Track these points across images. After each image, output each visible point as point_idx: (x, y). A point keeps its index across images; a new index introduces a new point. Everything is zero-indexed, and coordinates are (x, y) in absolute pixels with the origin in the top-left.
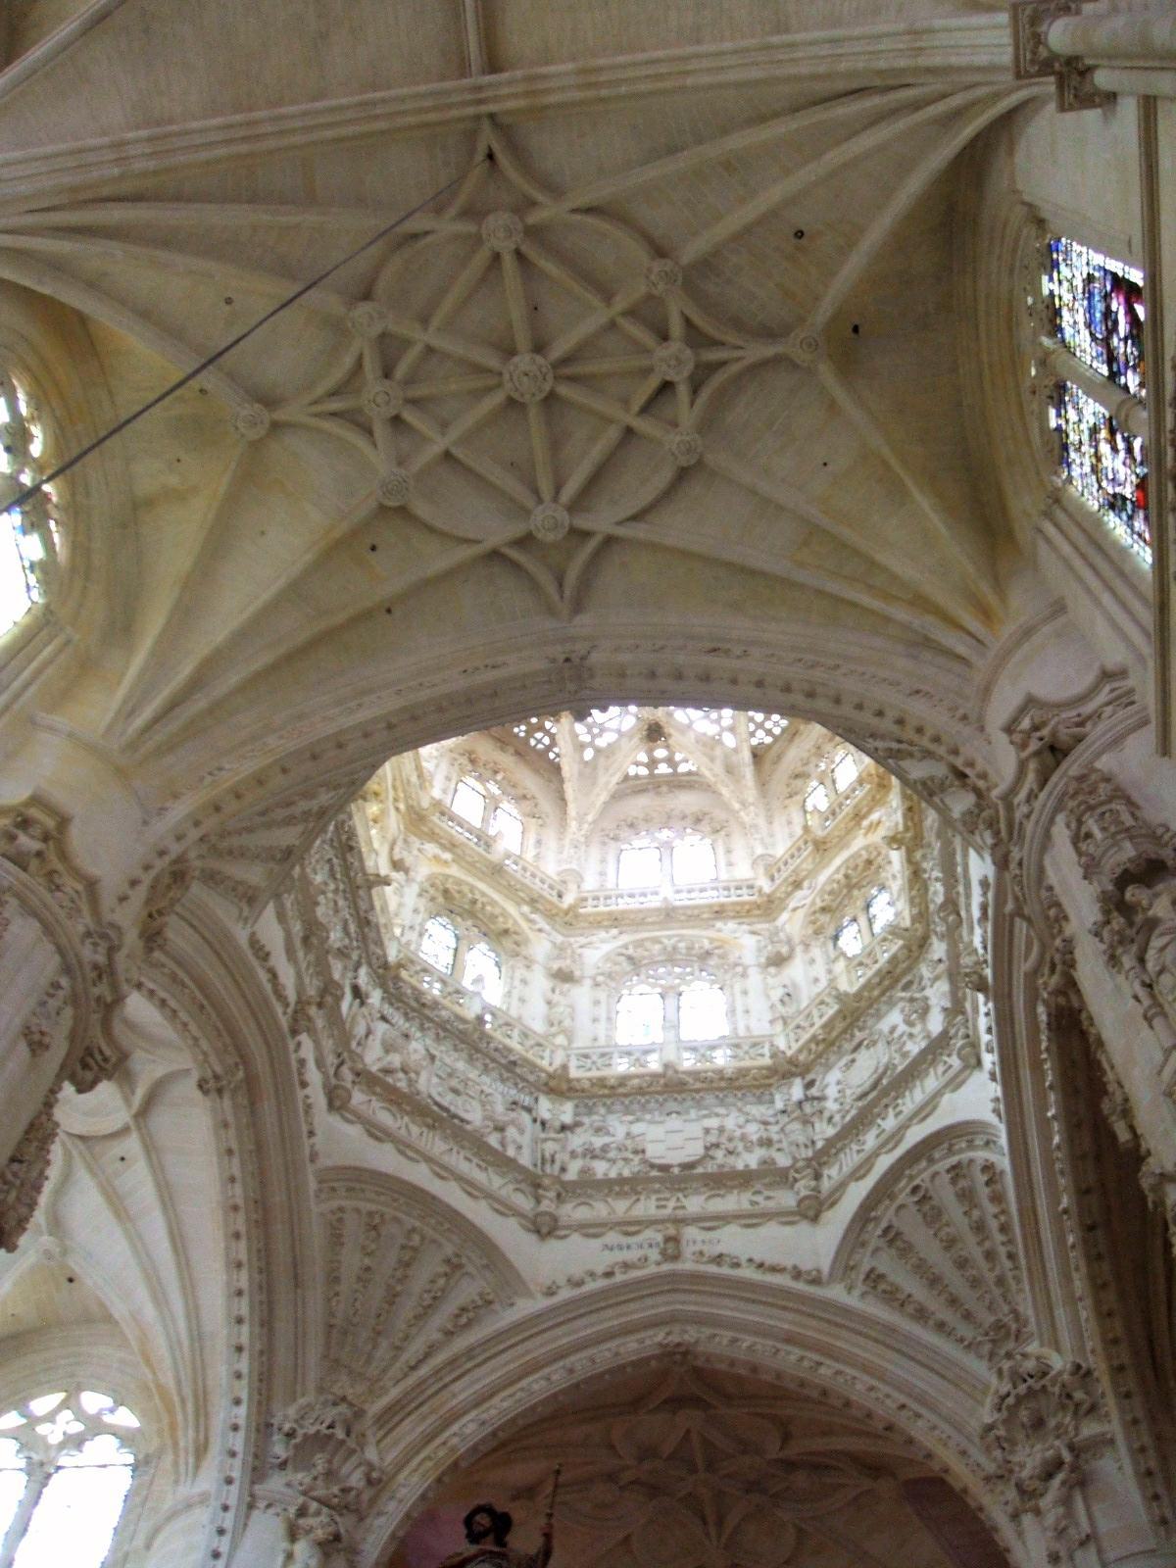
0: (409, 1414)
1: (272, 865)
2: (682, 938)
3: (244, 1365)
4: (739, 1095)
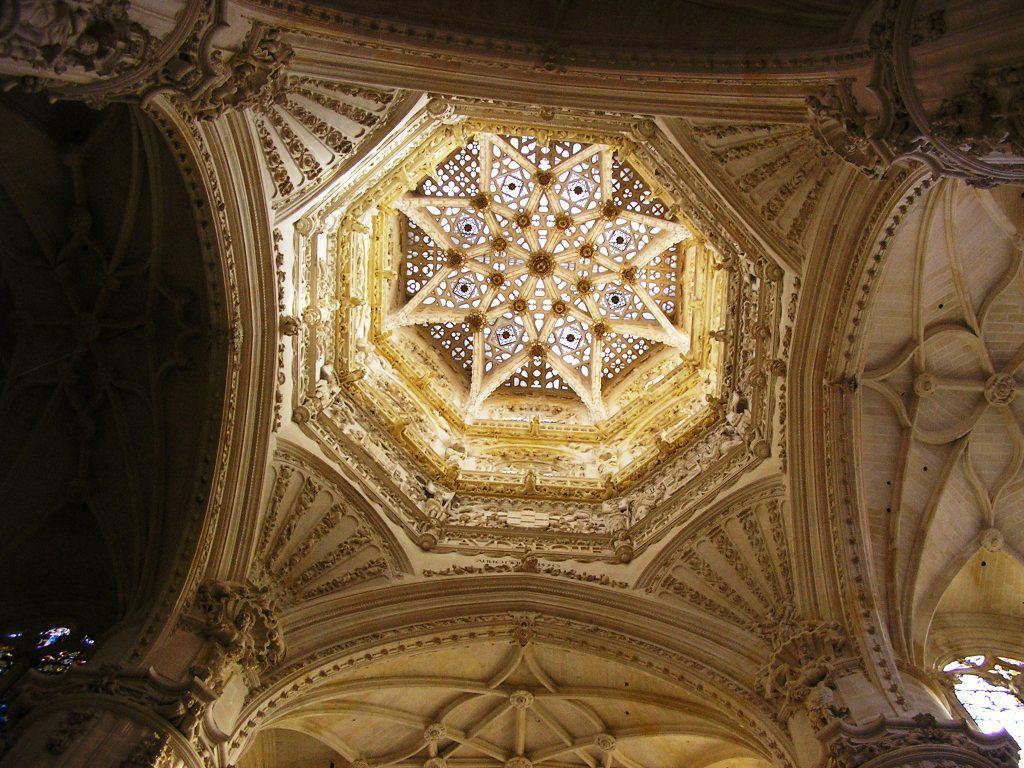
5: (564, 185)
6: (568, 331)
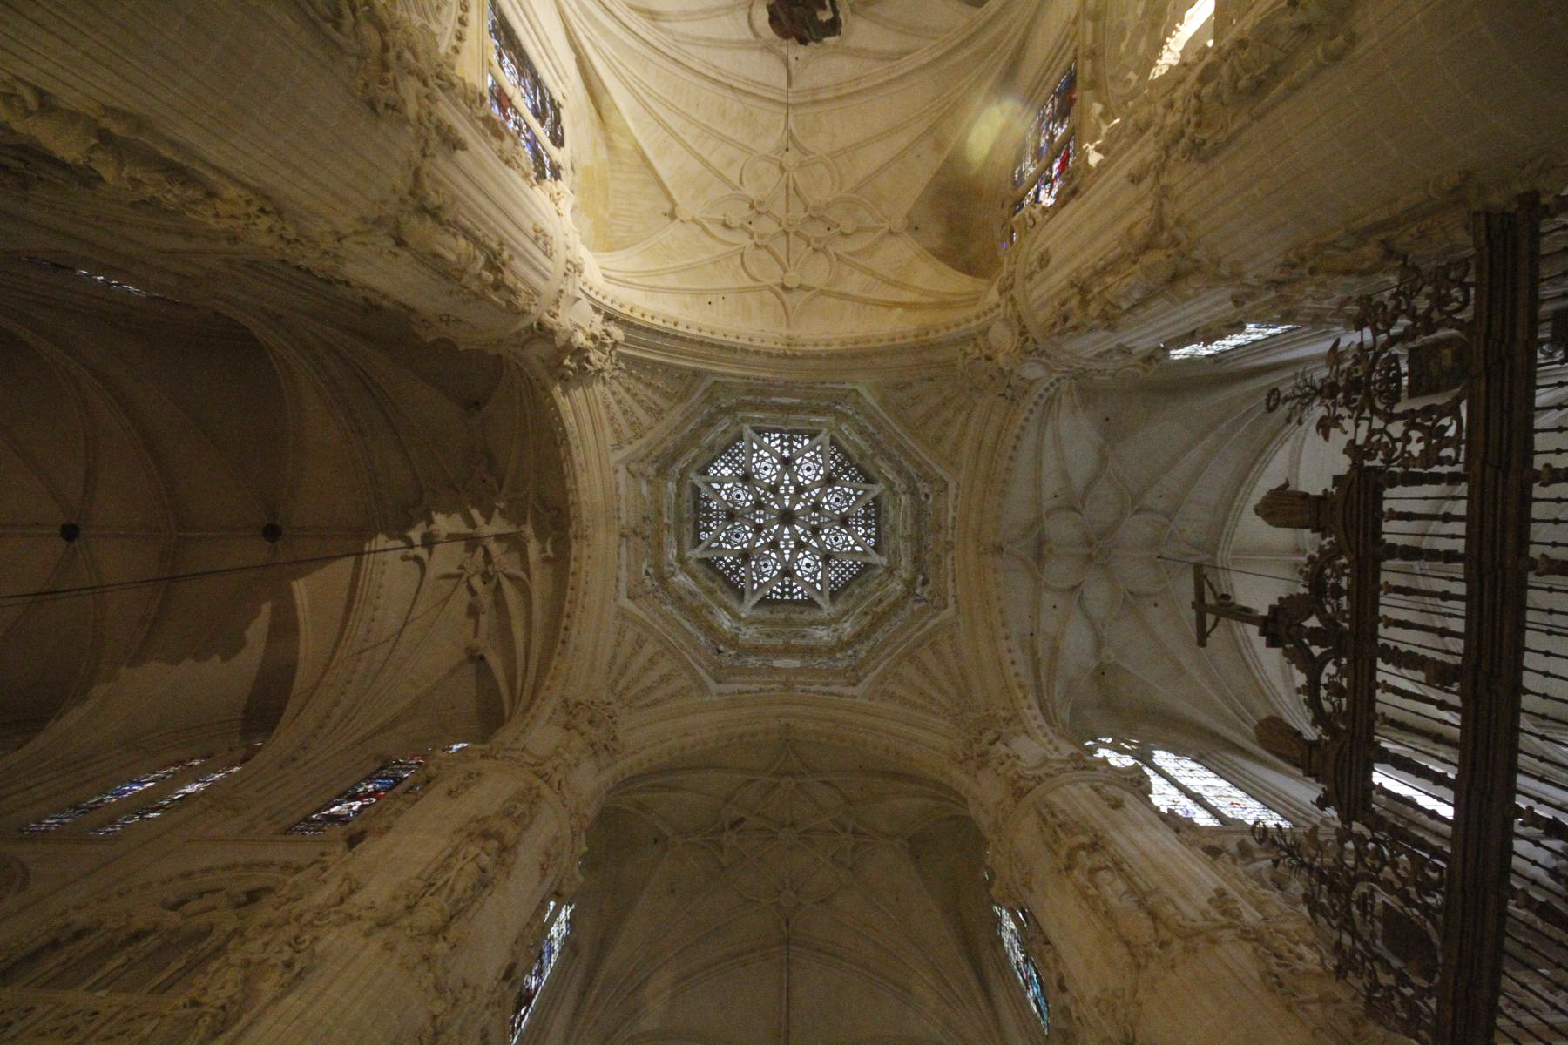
6: (806, 561)
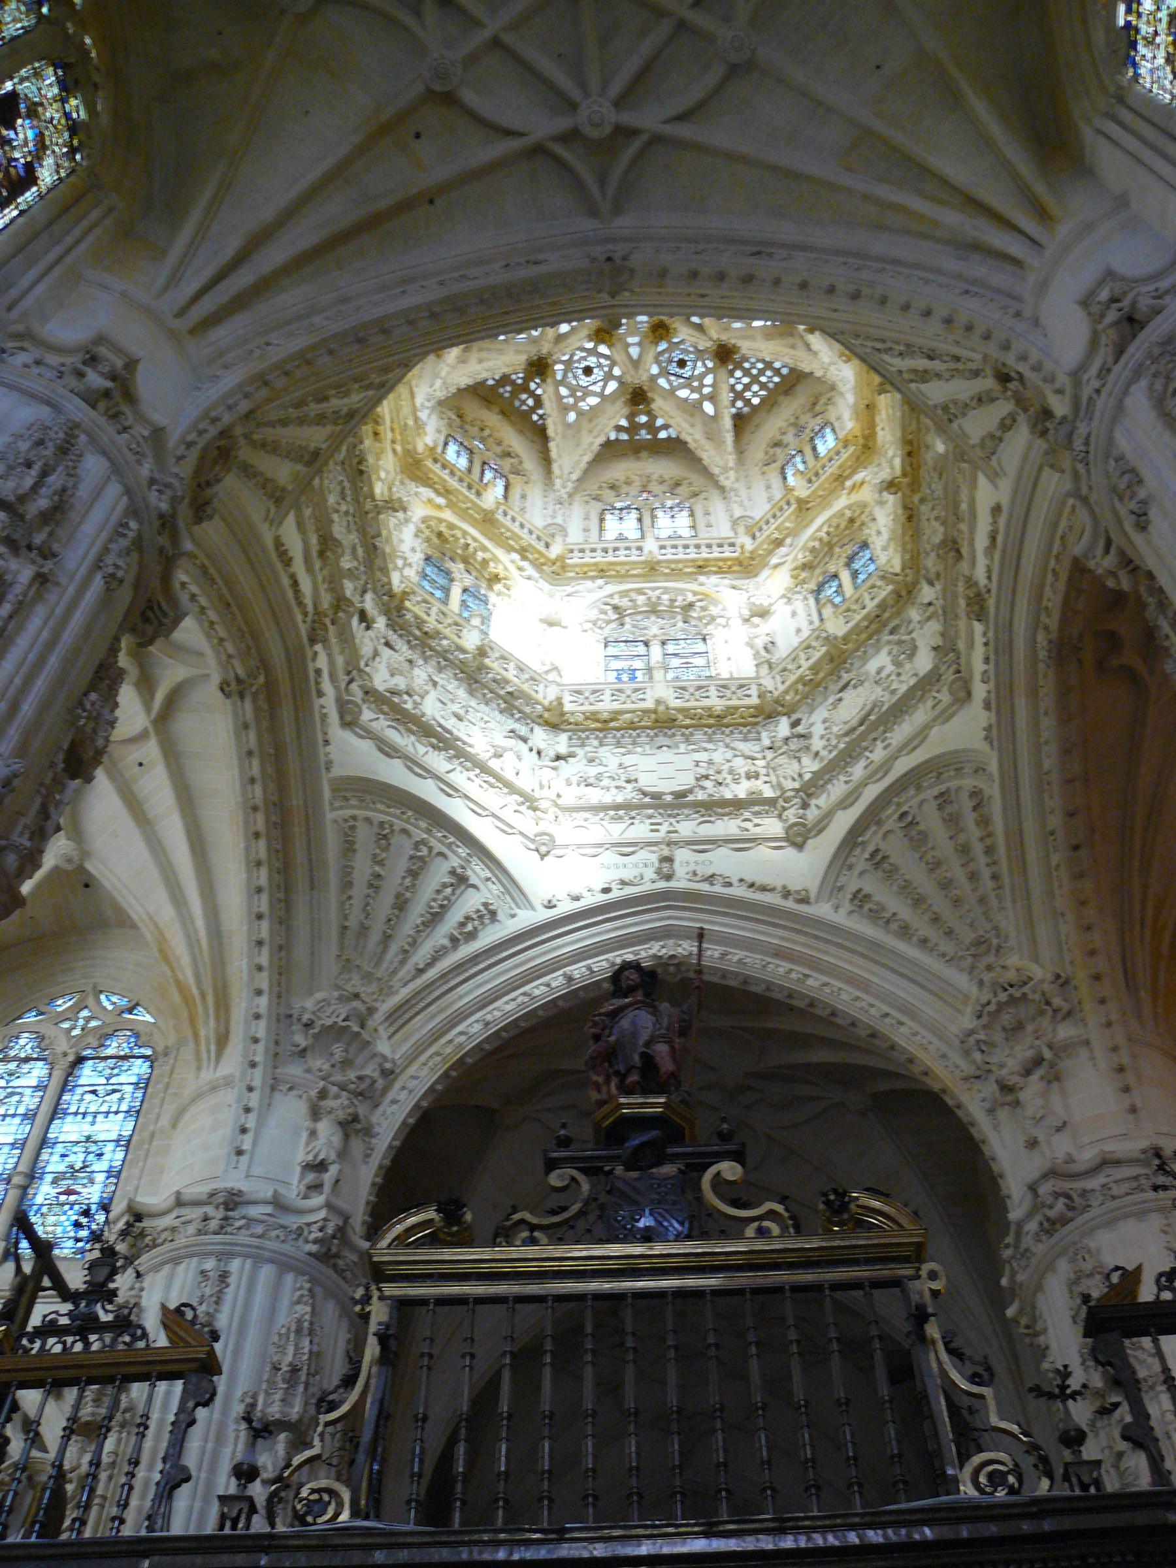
0: (417, 1014)
1: (299, 467)
2: (666, 590)
3: (264, 959)
4: (727, 731)
5: (608, 377)
